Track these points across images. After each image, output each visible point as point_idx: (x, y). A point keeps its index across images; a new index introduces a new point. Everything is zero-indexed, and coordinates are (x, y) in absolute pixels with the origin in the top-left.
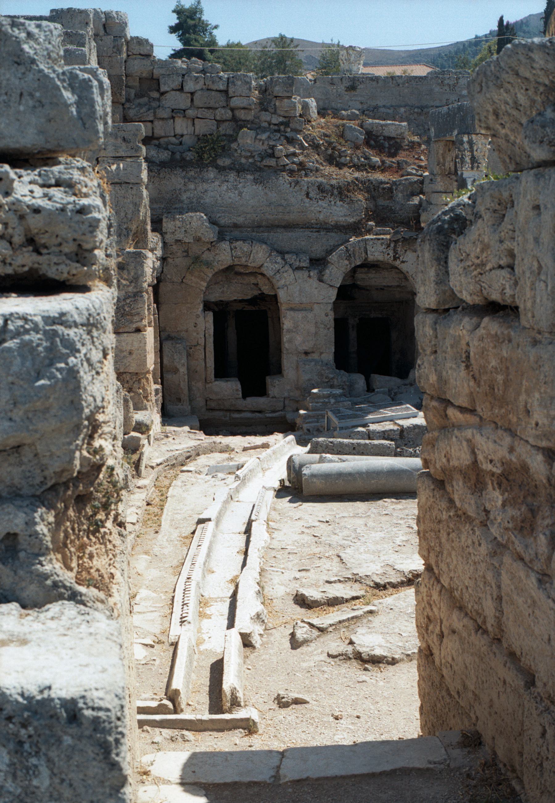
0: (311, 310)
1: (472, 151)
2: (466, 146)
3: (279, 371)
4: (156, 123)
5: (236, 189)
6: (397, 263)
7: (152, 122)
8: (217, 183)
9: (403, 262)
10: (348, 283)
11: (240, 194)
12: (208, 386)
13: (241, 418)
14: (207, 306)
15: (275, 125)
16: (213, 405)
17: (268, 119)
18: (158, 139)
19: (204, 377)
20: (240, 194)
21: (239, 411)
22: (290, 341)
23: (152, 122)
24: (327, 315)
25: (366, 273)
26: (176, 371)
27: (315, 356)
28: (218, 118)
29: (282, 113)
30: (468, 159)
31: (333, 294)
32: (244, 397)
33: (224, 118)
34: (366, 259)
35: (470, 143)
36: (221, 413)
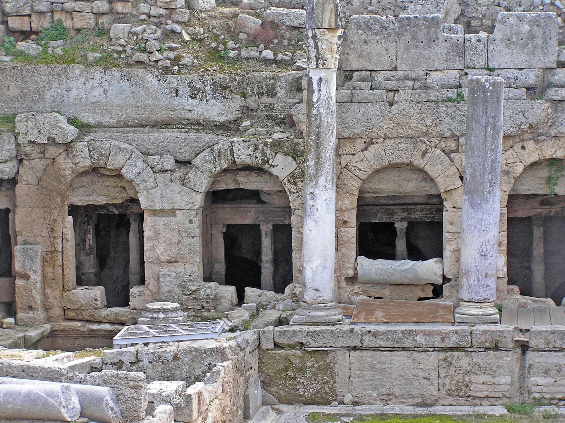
0: (175, 216)
1: (317, 47)
2: (311, 41)
3: (142, 281)
4: (33, 17)
5: (101, 87)
6: (267, 167)
7: (29, 16)
8: (82, 80)
9: (272, 166)
10: (222, 187)
11: (105, 91)
12: (65, 294)
13: (99, 330)
14: (73, 210)
15: (155, 17)
16: (71, 314)
17: (146, 11)
18: (37, 33)
19: (61, 284)
20: (105, 91)
21: (100, 322)
22: (153, 249)
23: (29, 16)
24: (191, 222)
25: (246, 176)
26: (26, 277)
27: (180, 268)
28: (95, 11)
29: (161, 4)
30: (313, 55)
31: (198, 200)
32: (108, 306)
33: (101, 11)
34: (235, 162)
35: (314, 37)
36: (79, 324)
